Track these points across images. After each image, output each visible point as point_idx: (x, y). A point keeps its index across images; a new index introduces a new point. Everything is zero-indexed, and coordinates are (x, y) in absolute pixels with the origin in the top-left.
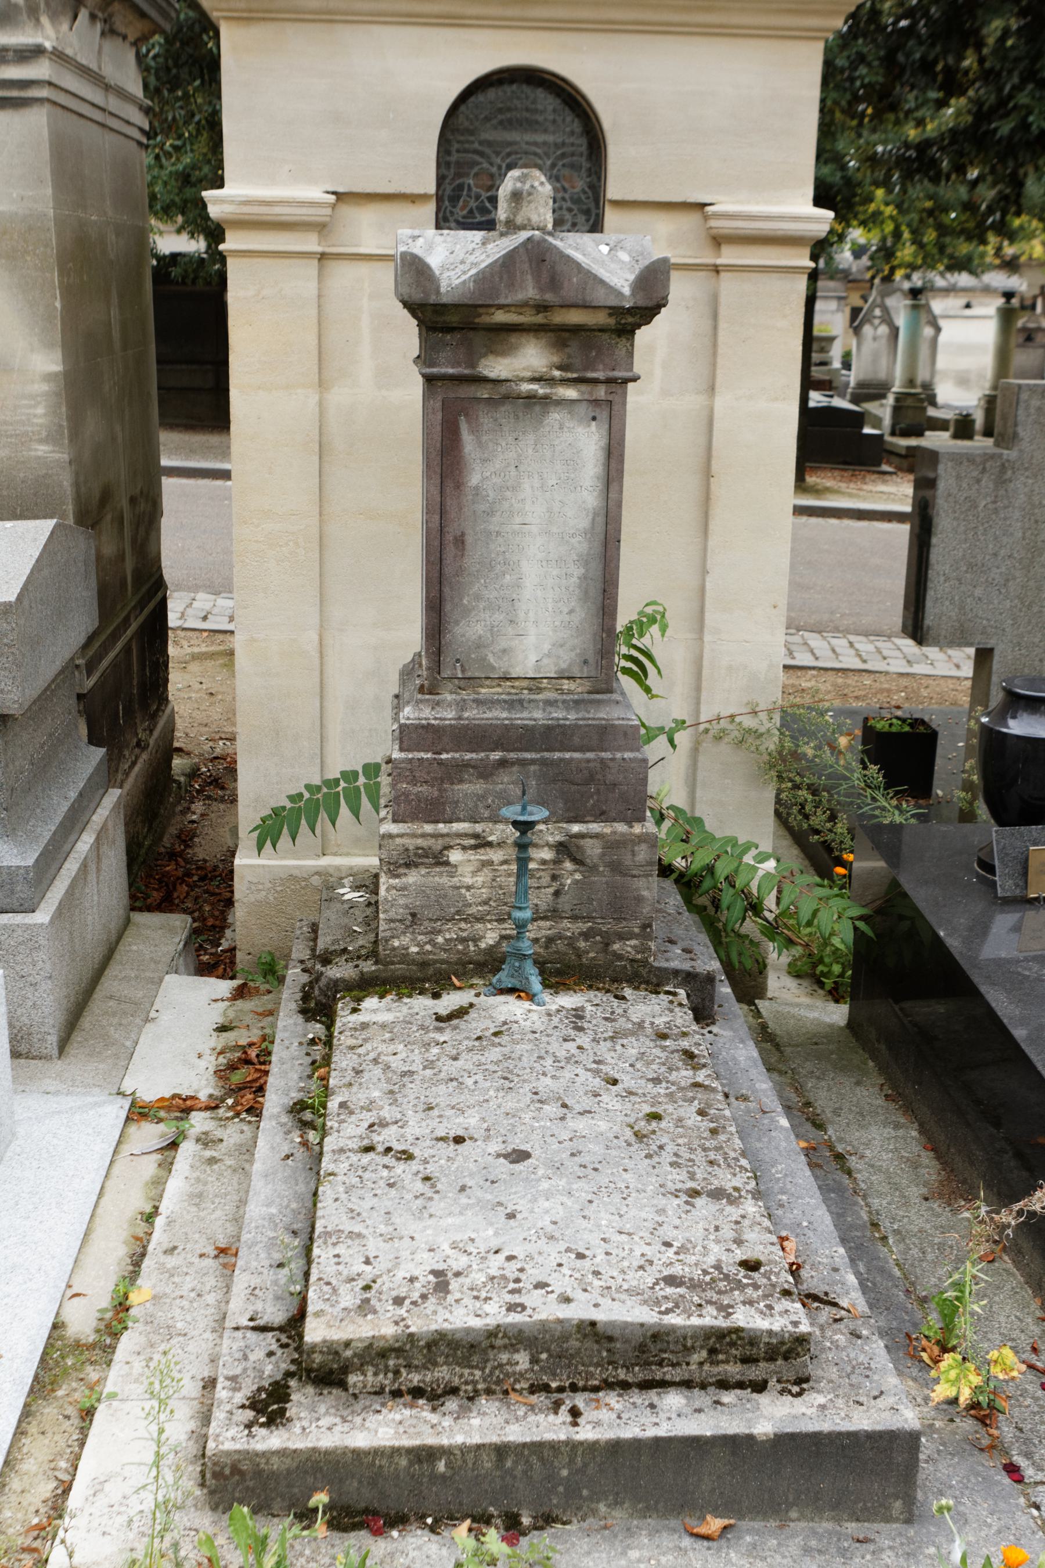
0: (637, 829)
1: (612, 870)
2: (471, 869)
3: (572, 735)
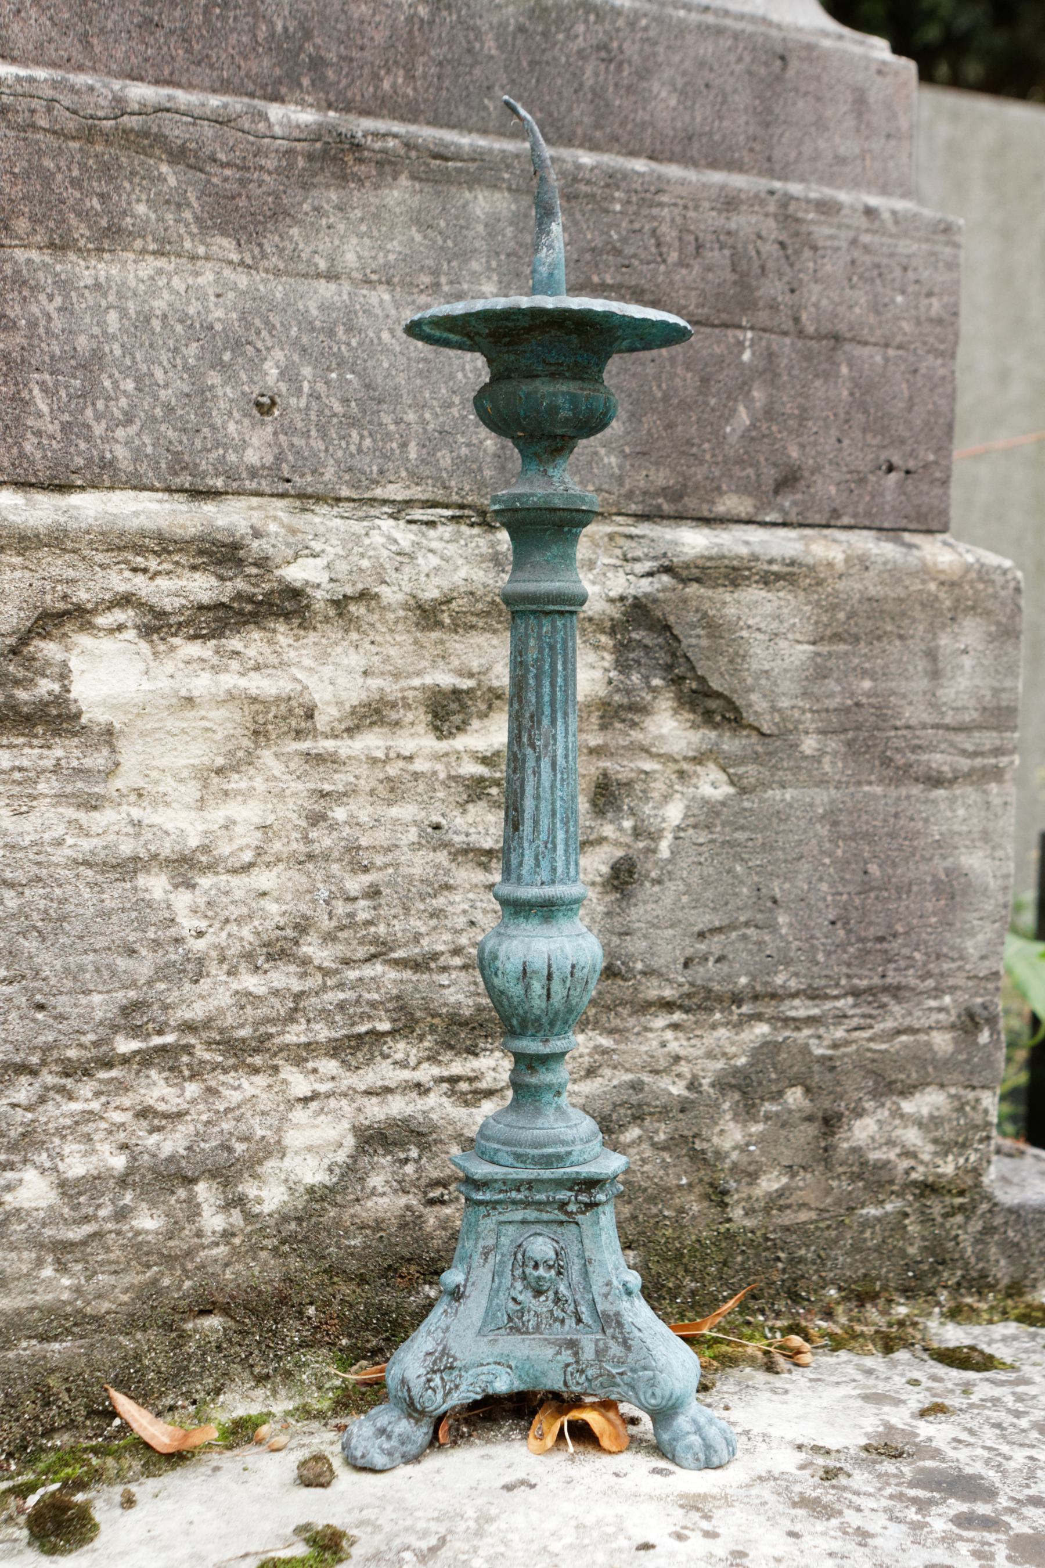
0: (940, 554)
1: (854, 750)
2: (198, 753)
3: (644, 74)
